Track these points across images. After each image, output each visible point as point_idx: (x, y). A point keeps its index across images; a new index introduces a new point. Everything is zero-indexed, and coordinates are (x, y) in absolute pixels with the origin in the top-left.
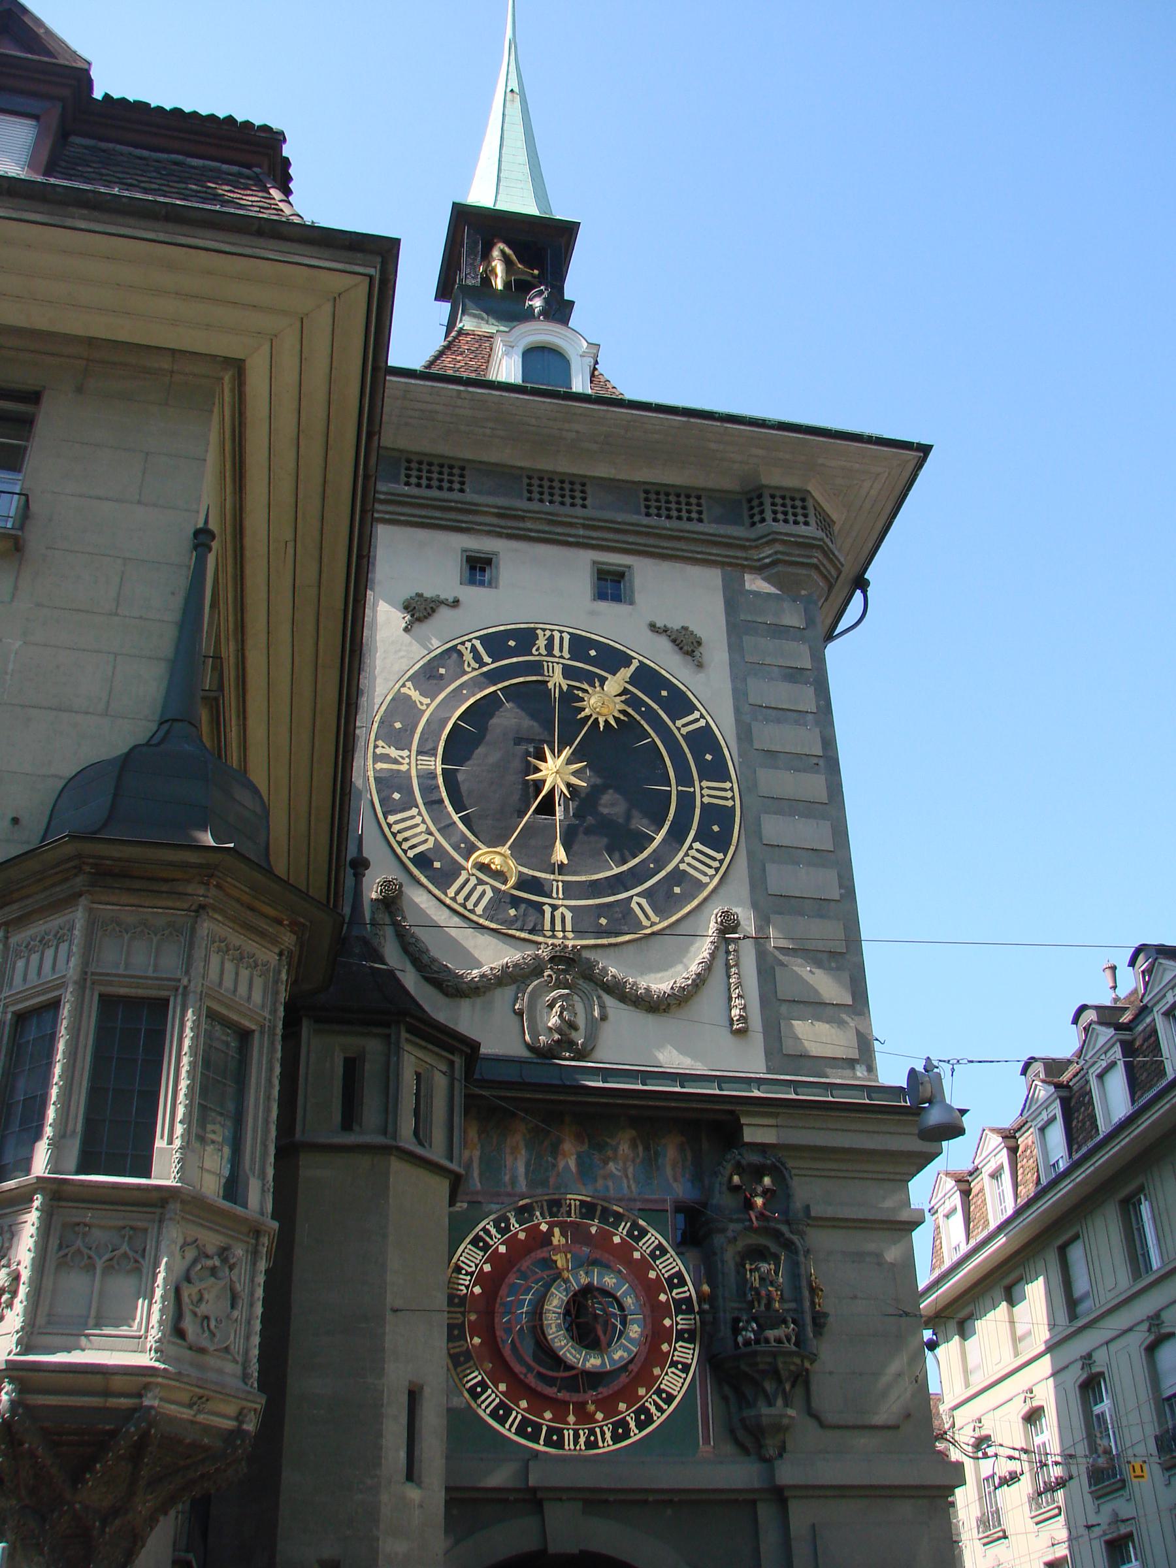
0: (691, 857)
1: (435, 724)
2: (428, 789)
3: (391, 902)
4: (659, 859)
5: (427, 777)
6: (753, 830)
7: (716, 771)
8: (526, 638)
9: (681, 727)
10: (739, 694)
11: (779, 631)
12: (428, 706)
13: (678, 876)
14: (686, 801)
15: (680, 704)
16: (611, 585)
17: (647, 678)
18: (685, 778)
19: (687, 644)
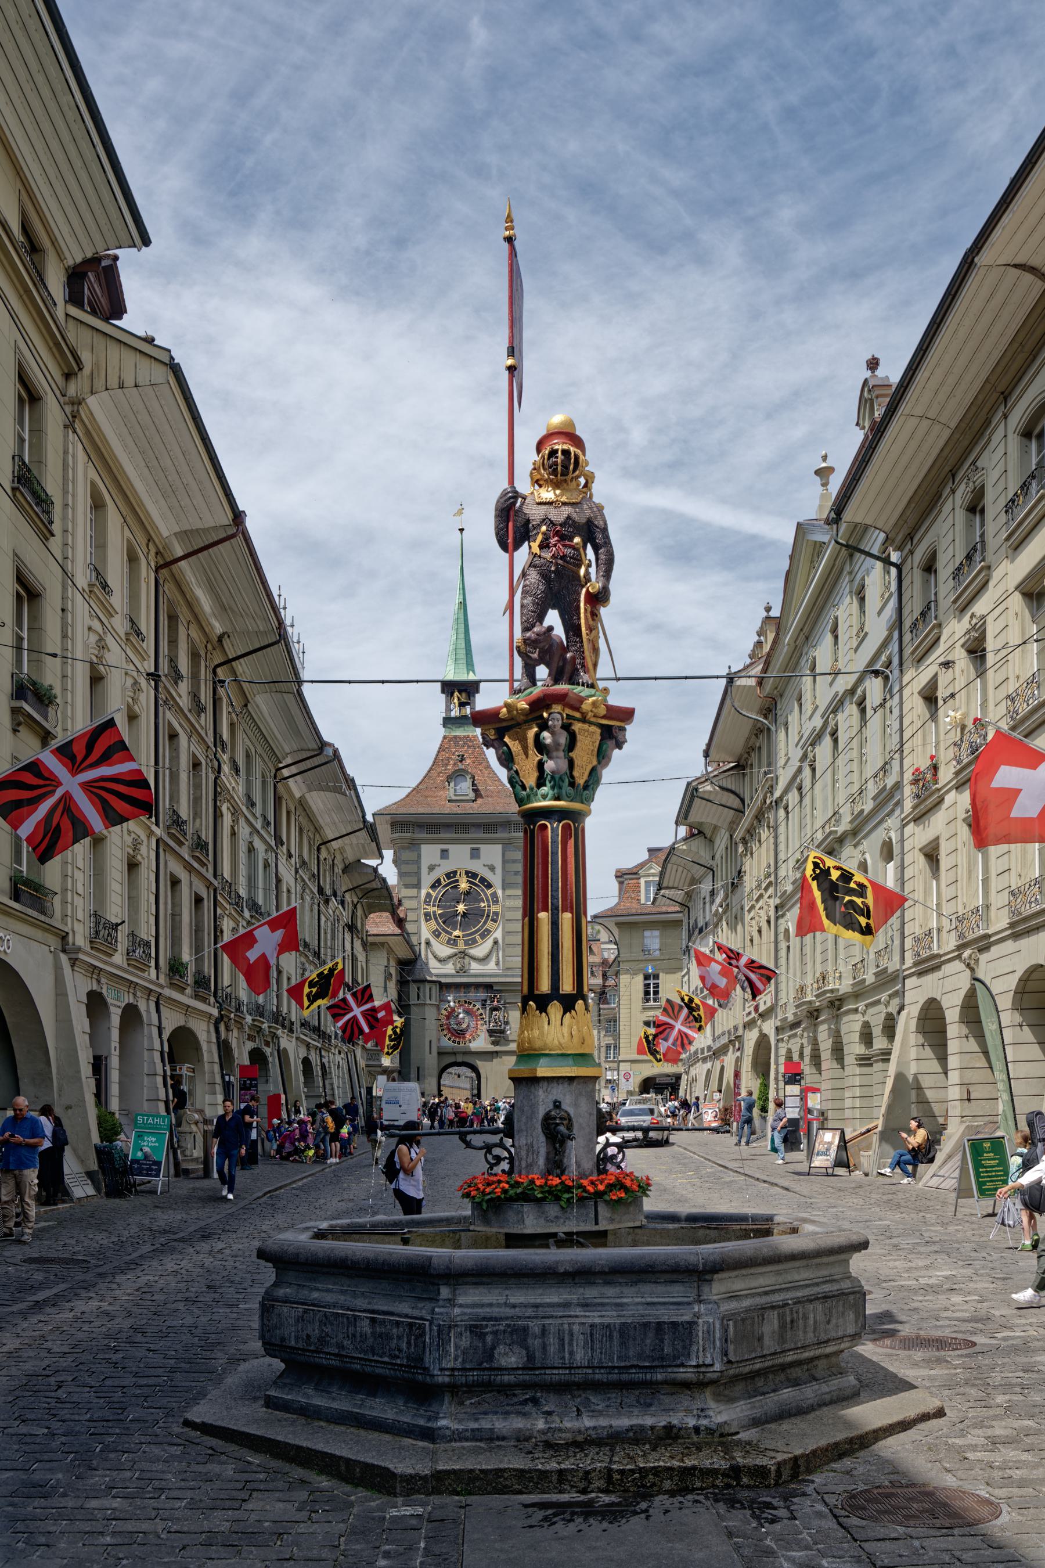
0: (489, 925)
1: (436, 898)
2: (435, 915)
3: (428, 943)
4: (482, 926)
5: (434, 912)
6: (503, 916)
7: (496, 902)
8: (455, 872)
9: (489, 892)
10: (503, 881)
11: (514, 861)
12: (434, 894)
13: (487, 930)
14: (489, 910)
15: (489, 886)
16: (475, 854)
17: (483, 880)
18: (489, 906)
19: (492, 868)
